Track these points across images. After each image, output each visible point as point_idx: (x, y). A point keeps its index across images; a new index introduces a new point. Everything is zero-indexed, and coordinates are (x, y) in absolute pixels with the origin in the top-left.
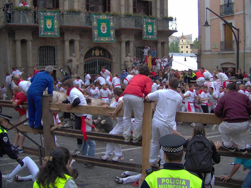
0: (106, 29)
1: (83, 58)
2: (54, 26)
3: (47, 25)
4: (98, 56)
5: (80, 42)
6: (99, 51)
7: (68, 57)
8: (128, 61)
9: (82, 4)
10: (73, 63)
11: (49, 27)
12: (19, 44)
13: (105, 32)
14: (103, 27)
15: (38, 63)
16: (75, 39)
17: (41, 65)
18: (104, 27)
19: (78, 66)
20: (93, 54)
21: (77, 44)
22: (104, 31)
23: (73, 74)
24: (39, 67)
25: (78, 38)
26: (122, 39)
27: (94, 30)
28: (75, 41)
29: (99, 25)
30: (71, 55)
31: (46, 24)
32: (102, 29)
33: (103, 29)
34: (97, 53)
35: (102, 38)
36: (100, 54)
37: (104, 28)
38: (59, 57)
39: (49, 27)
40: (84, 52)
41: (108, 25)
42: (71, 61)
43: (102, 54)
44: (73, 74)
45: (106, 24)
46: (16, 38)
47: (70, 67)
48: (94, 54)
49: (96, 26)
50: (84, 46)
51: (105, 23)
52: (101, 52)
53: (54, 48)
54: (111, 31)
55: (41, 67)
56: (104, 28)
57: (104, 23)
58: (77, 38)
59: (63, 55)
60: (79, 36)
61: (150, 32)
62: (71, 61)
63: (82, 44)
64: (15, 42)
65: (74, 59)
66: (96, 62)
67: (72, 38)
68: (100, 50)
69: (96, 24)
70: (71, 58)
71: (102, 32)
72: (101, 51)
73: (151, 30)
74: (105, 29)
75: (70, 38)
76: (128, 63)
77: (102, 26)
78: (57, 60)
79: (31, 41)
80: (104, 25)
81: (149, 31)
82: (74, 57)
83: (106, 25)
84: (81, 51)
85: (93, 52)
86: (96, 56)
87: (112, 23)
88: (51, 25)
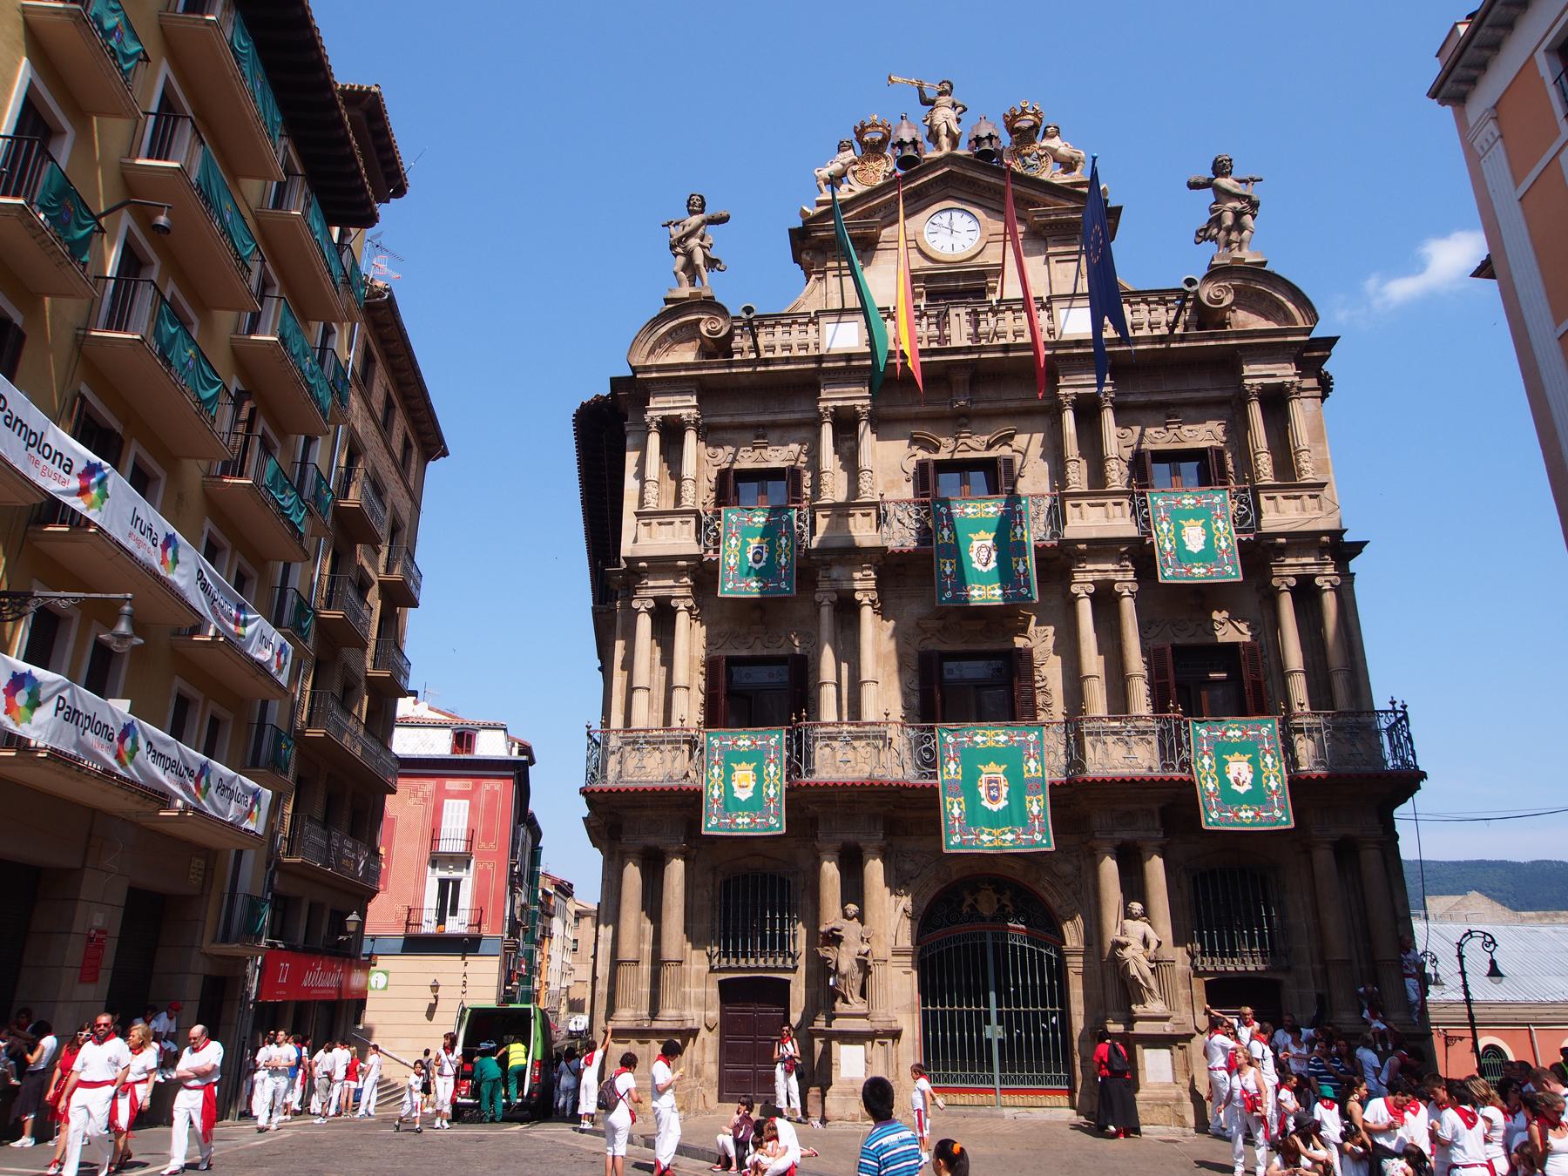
0: (1004, 791)
2: (765, 789)
3: (735, 785)
11: (743, 795)
13: (1003, 803)
14: (990, 781)
18: (996, 782)
20: (965, 909)
22: (994, 799)
23: (846, 1001)
27: (948, 799)
29: (971, 777)
31: (731, 781)
32: (982, 791)
33: (990, 789)
35: (987, 830)
37: (993, 784)
39: (743, 795)
41: (1014, 775)
44: (846, 1001)
45: (1004, 767)
48: (972, 907)
49: (957, 781)
51: (998, 763)
54: (1028, 798)
56: (993, 784)
57: (992, 767)
61: (1242, 790)
66: (984, 946)
68: (999, 890)
69: (956, 773)
71: (985, 803)
72: (1008, 893)
73: (1250, 777)
74: (998, 789)
77: (983, 777)
80: (993, 771)
81: (1235, 787)
83: (1004, 772)
85: (969, 900)
86: (983, 919)
87: (1032, 763)
88: (752, 784)
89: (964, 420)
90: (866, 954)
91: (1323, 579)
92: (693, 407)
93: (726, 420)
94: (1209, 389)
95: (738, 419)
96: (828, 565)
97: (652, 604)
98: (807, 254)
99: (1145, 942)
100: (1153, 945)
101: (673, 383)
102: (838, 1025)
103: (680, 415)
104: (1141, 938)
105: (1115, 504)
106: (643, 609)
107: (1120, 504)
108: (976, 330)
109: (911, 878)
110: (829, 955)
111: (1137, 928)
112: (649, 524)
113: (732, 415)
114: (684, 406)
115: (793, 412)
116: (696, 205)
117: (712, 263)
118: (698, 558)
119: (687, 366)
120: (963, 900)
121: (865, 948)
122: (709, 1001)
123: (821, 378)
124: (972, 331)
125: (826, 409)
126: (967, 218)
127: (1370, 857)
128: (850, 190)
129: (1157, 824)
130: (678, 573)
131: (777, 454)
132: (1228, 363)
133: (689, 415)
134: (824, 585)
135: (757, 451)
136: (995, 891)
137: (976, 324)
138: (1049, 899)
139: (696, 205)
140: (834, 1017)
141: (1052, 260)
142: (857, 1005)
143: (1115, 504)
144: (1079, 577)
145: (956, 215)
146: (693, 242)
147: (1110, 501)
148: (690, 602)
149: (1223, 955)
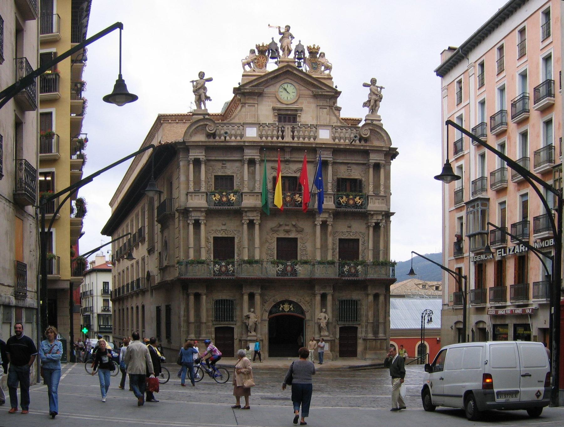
1: (267, 314)
4: (288, 312)
5: (261, 295)
6: (289, 306)
7: (246, 312)
8: (321, 319)
9: (268, 249)
10: (250, 320)
12: (192, 298)
15: (214, 319)
16: (255, 292)
17: (217, 321)
19: (256, 323)
20: (281, 309)
21: (258, 298)
23: (251, 333)
24: (214, 323)
25: (259, 291)
26: (316, 292)
28: (255, 294)
30: (249, 311)
34: (286, 307)
36: (290, 309)
38: (237, 313)
40: (268, 307)
42: (249, 318)
43: (292, 309)
44: (251, 333)
46: (189, 291)
47: (247, 324)
50: (268, 300)
52: (291, 306)
53: (232, 301)
55: (216, 323)
58: (257, 292)
59: (242, 310)
60: (260, 289)
62: (248, 317)
63: (266, 298)
64: (188, 295)
65: (252, 315)
67: (252, 291)
70: (248, 314)
75: (249, 291)
76: (321, 321)
78: (236, 317)
79: (205, 294)
82: (252, 312)
84: (264, 306)
85: (282, 306)
86: (285, 312)
89: (287, 163)
90: (256, 321)
91: (382, 224)
92: (203, 155)
93: (213, 158)
94: (361, 160)
95: (217, 158)
96: (246, 212)
97: (193, 222)
98: (239, 96)
99: (325, 318)
100: (327, 319)
101: (197, 146)
102: (249, 338)
103: (200, 158)
104: (324, 317)
105: (330, 197)
106: (191, 223)
107: (331, 197)
108: (293, 134)
109: (267, 301)
110: (247, 321)
111: (323, 315)
112: (192, 196)
113: (215, 157)
114: (200, 155)
115: (234, 157)
116: (202, 75)
117: (208, 98)
118: (208, 208)
119: (202, 142)
120: (280, 307)
121: (256, 320)
122: (212, 332)
123: (244, 147)
124: (292, 134)
125: (246, 159)
126: (293, 87)
127: (382, 298)
128: (254, 71)
129: (332, 289)
130: (202, 212)
131: (229, 170)
132: (366, 153)
133: (203, 159)
134: (245, 218)
135: (223, 169)
136: (289, 304)
137: (293, 132)
138: (303, 308)
139: (202, 75)
140: (248, 336)
141: (319, 108)
142: (253, 333)
143: (330, 197)
144: (317, 219)
145: (289, 85)
146: (202, 91)
147: (328, 196)
148: (205, 221)
149: (347, 321)
